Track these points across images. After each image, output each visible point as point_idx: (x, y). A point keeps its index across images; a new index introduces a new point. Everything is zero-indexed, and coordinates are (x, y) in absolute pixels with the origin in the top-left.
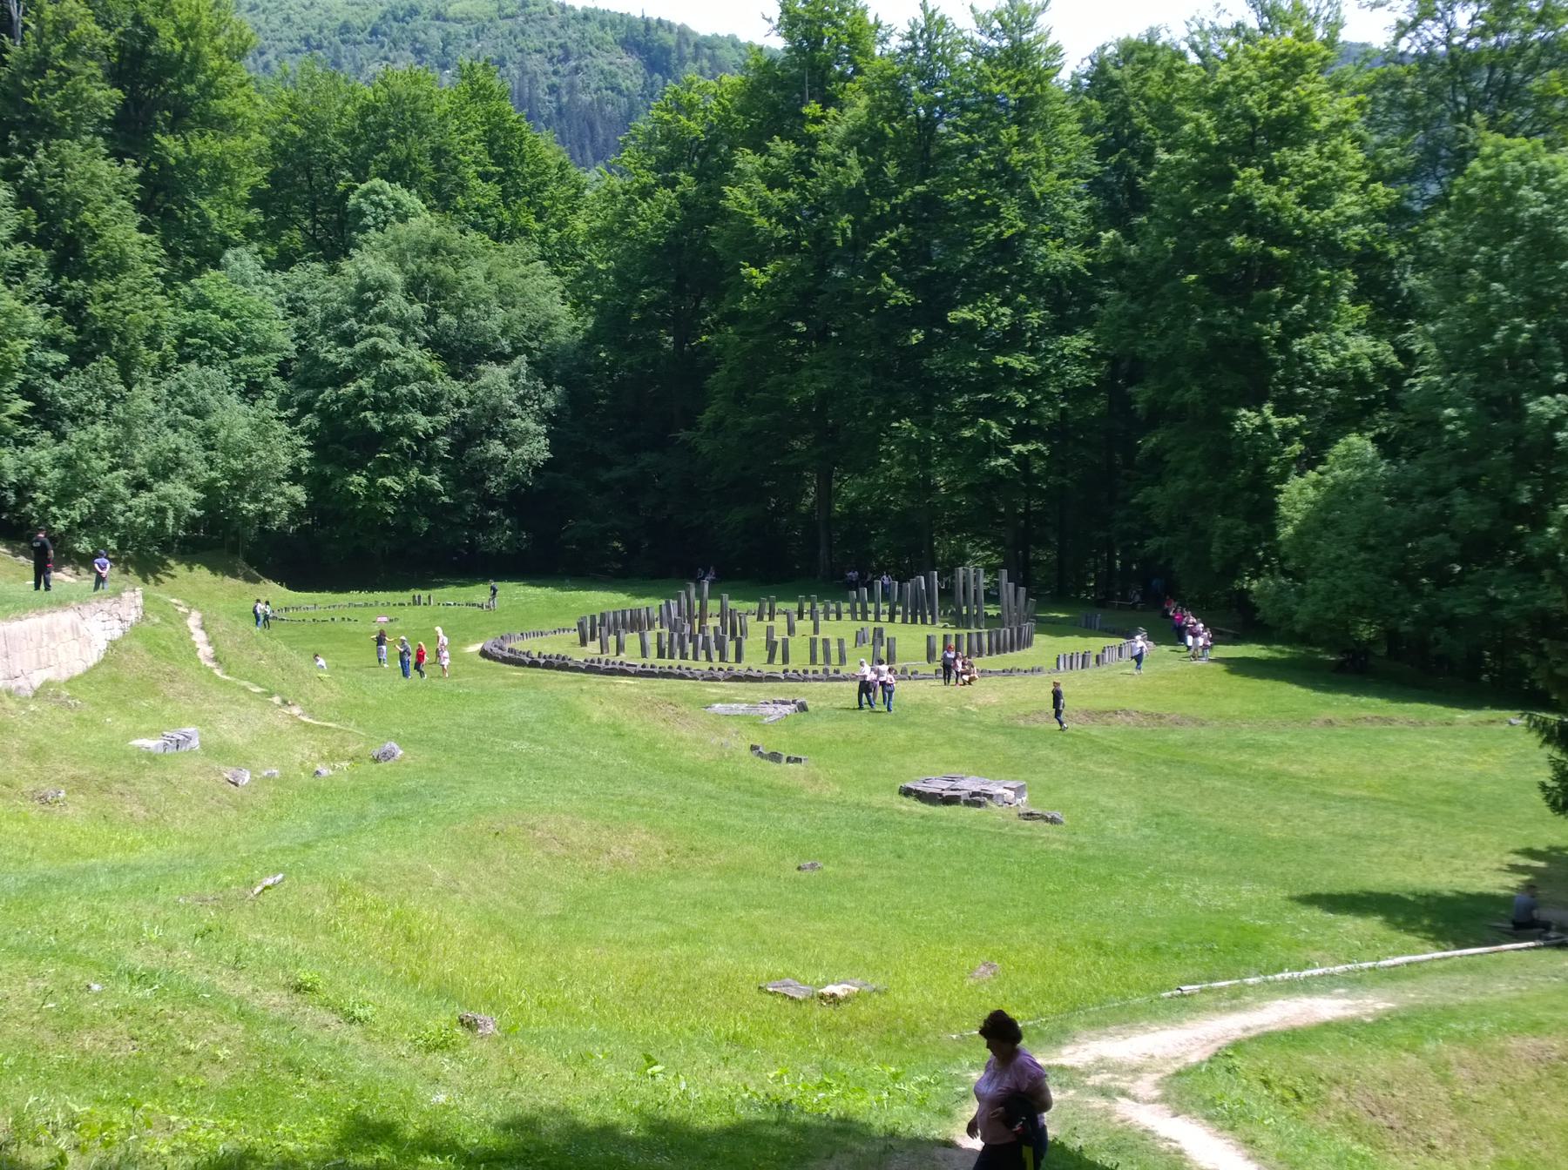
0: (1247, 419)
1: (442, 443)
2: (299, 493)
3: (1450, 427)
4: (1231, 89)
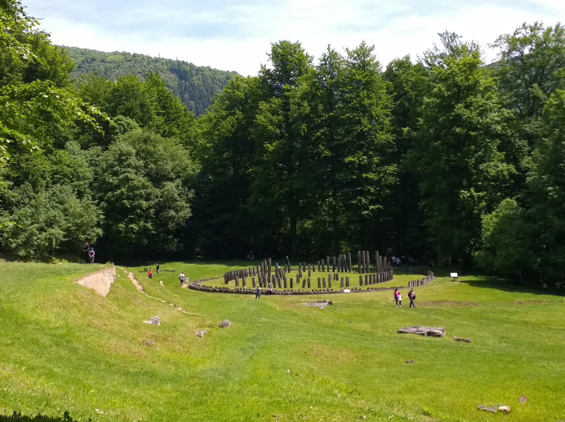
0: (465, 194)
1: (152, 211)
2: (100, 231)
3: (551, 194)
4: (450, 76)
